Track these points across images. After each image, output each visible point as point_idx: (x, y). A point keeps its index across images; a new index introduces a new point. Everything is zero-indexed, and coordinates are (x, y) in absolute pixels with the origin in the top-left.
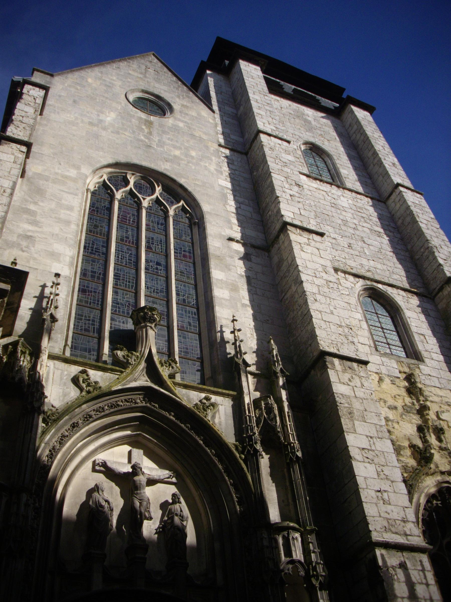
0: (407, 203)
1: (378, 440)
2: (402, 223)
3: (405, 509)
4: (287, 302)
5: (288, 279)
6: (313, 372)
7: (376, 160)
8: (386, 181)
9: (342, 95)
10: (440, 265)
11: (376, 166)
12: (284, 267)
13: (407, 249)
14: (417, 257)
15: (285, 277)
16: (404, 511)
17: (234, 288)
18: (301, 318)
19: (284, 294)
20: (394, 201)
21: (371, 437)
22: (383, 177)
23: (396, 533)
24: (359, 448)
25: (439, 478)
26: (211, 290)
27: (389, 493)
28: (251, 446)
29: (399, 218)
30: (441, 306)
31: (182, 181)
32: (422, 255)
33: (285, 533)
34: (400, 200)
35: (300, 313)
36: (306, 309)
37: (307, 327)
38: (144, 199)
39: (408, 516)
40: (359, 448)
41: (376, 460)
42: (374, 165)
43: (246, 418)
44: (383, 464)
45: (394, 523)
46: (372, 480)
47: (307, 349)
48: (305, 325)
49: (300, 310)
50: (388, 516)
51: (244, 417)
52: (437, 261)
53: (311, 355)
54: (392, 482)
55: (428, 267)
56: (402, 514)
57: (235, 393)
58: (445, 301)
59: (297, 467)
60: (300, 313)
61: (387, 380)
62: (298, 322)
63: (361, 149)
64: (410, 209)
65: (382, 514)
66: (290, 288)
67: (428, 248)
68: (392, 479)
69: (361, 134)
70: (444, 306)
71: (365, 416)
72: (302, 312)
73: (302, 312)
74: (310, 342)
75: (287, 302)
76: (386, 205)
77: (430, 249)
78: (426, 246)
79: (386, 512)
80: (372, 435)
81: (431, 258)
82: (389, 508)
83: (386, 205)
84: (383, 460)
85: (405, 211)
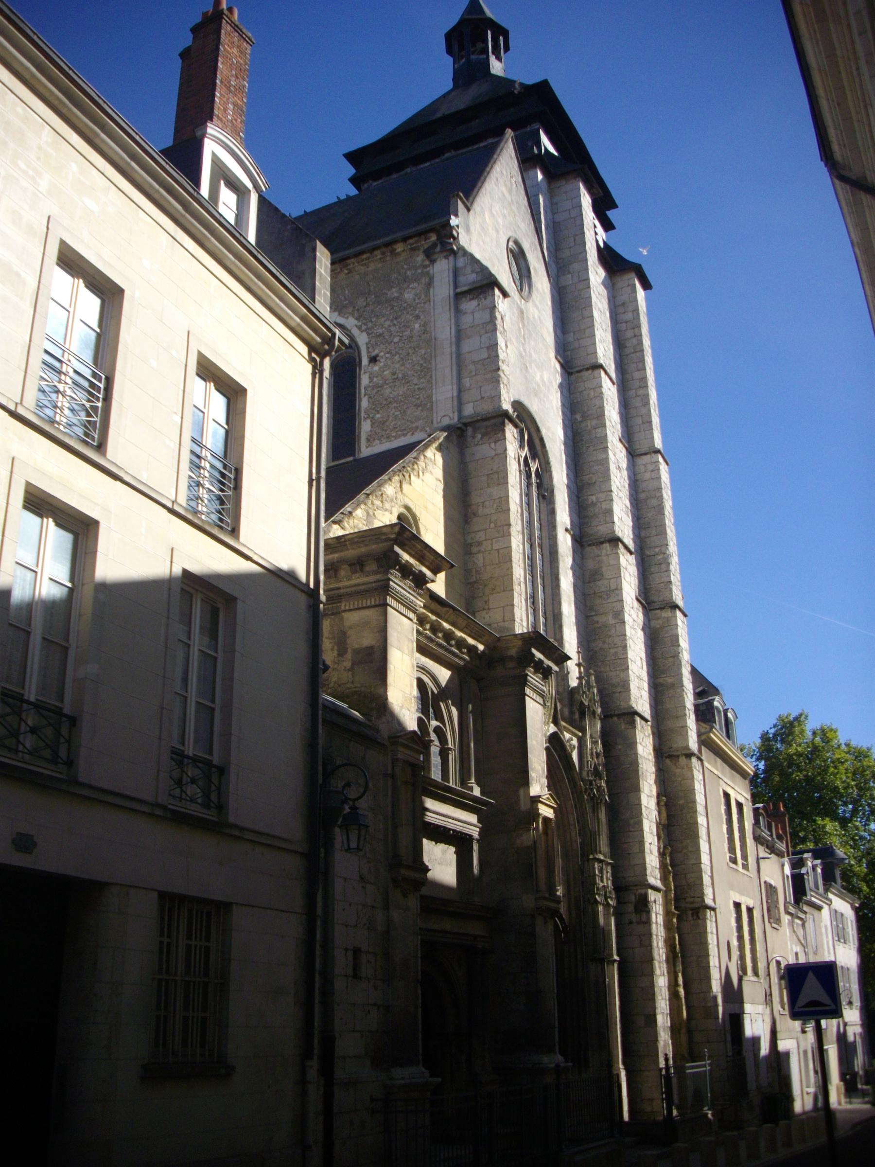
0: (660, 483)
2: (645, 500)
4: (596, 625)
5: (604, 602)
6: (615, 719)
7: (641, 392)
8: (644, 431)
9: (609, 210)
10: (671, 582)
11: (639, 399)
12: (602, 585)
13: (640, 534)
14: (648, 553)
15: (601, 597)
17: (569, 603)
18: (613, 658)
19: (593, 613)
20: (645, 465)
22: (643, 423)
26: (560, 604)
28: (592, 790)
29: (644, 491)
30: (653, 623)
31: (544, 432)
32: (654, 555)
33: (601, 865)
34: (652, 471)
35: (613, 651)
36: (623, 654)
37: (618, 672)
42: (637, 396)
43: (588, 762)
47: (614, 693)
48: (618, 669)
49: (613, 648)
51: (585, 760)
52: (669, 576)
53: (618, 702)
55: (657, 575)
57: (580, 734)
58: (660, 621)
59: (603, 809)
60: (613, 651)
62: (608, 658)
63: (627, 355)
64: (661, 492)
66: (605, 614)
67: (665, 553)
69: (635, 336)
70: (658, 626)
72: (616, 653)
73: (616, 653)
74: (619, 689)
75: (596, 625)
76: (633, 461)
77: (665, 555)
78: (663, 549)
81: (663, 566)
83: (633, 461)
85: (654, 490)
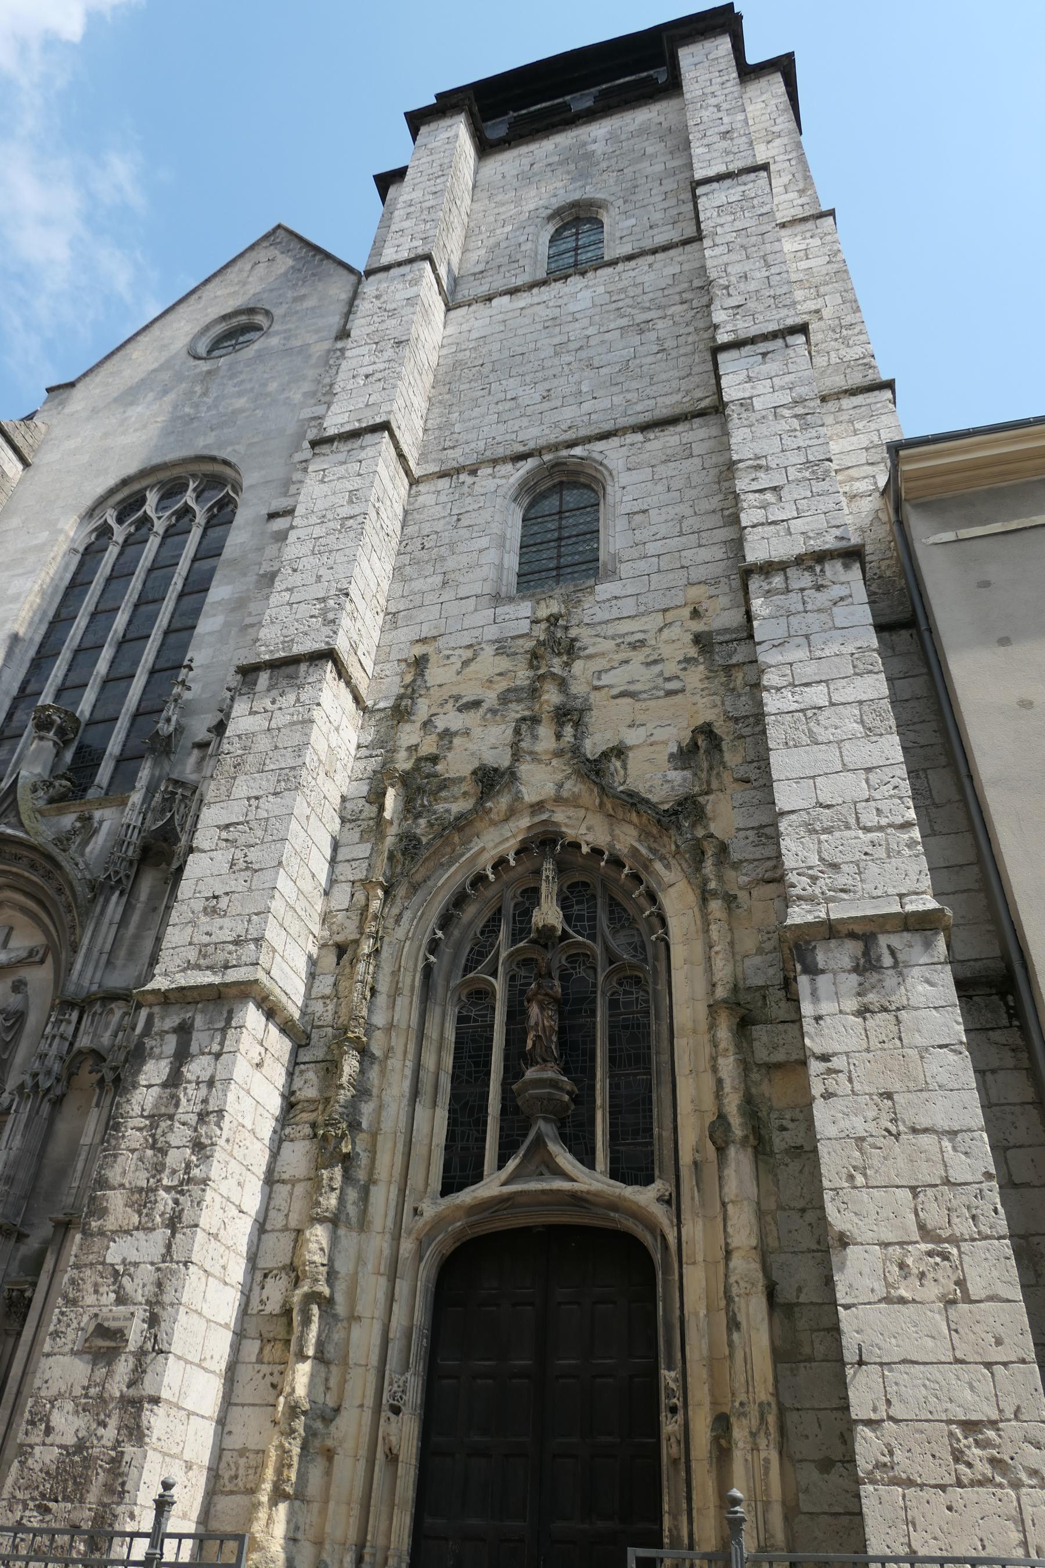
1: (271, 798)
3: (254, 917)
16: (249, 921)
21: (257, 798)
23: (208, 968)
24: (218, 827)
25: (525, 822)
27: (234, 896)
38: (159, 518)
39: (251, 931)
40: (218, 827)
41: (242, 840)
44: (252, 841)
45: (210, 949)
46: (210, 880)
50: (206, 939)
54: (256, 871)
56: (240, 930)
61: (489, 650)
65: (195, 940)
68: (256, 867)
71: (268, 761)
79: (207, 934)
80: (256, 793)
82: (218, 921)
84: (260, 833)
